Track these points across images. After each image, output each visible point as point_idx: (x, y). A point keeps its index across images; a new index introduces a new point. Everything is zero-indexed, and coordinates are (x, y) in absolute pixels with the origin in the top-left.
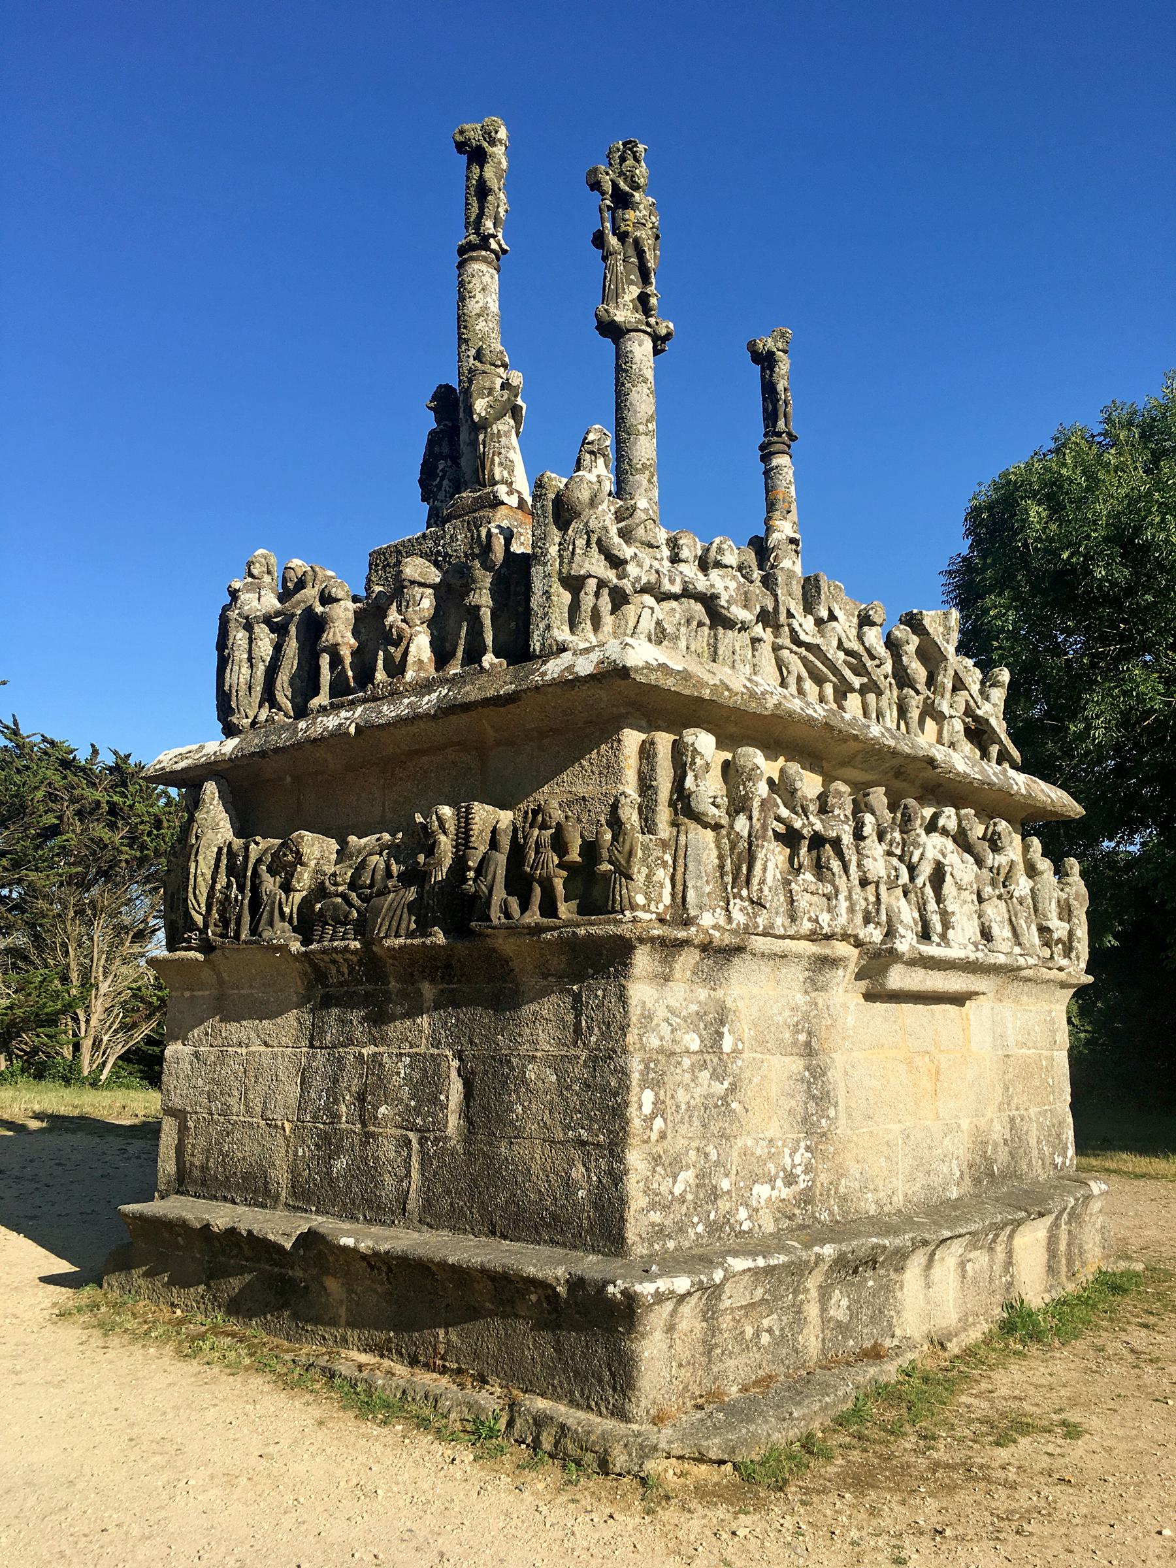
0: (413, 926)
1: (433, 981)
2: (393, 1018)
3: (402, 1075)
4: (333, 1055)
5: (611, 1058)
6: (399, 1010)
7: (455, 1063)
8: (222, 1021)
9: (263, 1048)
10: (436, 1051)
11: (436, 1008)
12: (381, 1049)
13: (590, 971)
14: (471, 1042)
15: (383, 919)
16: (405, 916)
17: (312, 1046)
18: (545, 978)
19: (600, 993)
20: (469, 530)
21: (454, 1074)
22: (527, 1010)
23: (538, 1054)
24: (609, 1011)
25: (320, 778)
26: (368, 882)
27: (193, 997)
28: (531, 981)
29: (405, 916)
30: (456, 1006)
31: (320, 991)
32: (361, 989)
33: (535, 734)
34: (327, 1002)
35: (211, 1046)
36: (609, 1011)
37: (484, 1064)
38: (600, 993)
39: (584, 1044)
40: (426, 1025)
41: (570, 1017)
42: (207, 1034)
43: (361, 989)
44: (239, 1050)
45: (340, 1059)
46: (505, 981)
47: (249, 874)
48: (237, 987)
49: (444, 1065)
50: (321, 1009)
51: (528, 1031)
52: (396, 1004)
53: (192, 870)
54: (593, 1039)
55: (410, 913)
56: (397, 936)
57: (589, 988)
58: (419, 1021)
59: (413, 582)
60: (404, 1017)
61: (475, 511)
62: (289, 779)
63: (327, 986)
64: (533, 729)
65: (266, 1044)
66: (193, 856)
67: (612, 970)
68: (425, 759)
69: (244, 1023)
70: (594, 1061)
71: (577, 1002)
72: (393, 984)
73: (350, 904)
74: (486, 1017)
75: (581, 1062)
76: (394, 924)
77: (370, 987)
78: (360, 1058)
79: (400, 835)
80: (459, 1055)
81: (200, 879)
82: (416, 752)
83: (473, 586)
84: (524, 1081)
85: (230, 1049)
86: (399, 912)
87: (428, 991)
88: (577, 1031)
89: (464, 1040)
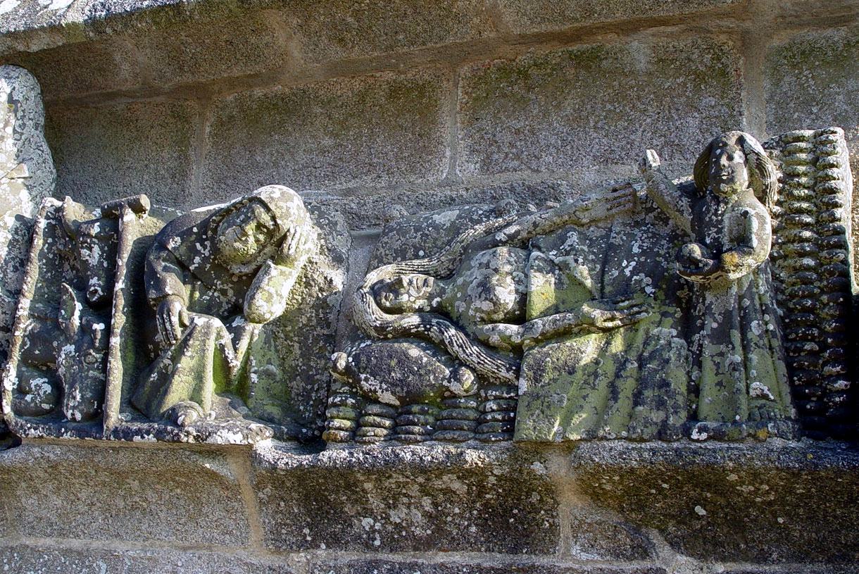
73: (456, 363)
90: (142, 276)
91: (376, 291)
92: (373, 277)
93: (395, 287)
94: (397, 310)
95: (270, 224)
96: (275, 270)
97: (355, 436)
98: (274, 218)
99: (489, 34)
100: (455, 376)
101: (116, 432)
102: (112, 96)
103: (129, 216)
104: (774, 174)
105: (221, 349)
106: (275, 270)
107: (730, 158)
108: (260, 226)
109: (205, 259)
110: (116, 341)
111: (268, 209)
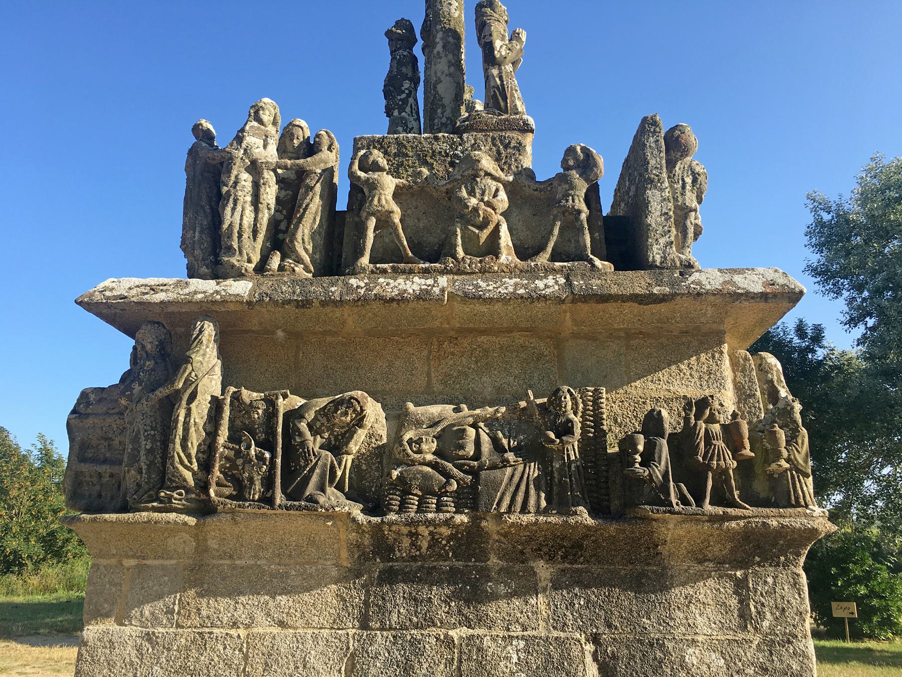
0: (544, 504)
1: (551, 559)
2: (494, 597)
3: (515, 659)
4: (403, 637)
5: (789, 642)
6: (502, 589)
7: (589, 648)
8: (200, 595)
9: (276, 630)
10: (562, 635)
11: (556, 586)
12: (478, 631)
13: (757, 559)
14: (610, 626)
15: (503, 494)
16: (532, 492)
17: (364, 626)
18: (700, 562)
19: (770, 580)
20: (494, 145)
21: (589, 659)
22: (677, 593)
23: (700, 638)
24: (783, 598)
25: (329, 339)
26: (472, 453)
27: (140, 568)
28: (679, 565)
29: (532, 492)
30: (586, 586)
31: (379, 565)
32: (445, 565)
33: (622, 334)
34: (389, 577)
35: (179, 626)
36: (783, 598)
37: (628, 647)
38: (770, 580)
39: (756, 629)
40: (543, 607)
41: (734, 602)
42: (172, 612)
43: (445, 565)
44: (233, 632)
45: (414, 642)
46: (648, 564)
47: (280, 430)
48: (231, 557)
49: (575, 651)
50: (380, 585)
51: (681, 615)
52: (498, 582)
53: (181, 418)
54: (766, 624)
55: (538, 489)
56: (524, 510)
57: (755, 573)
58: (533, 601)
59: (488, 174)
60: (509, 596)
61: (502, 130)
62: (280, 334)
63: (392, 560)
64: (620, 329)
65: (282, 624)
66: (184, 403)
67: (782, 558)
68: (483, 339)
69: (242, 599)
70: (770, 645)
71: (740, 586)
72: (494, 561)
73: (448, 476)
74: (626, 599)
75: (754, 646)
76: (520, 499)
77: (460, 564)
78: (449, 642)
79: (503, 409)
80: (595, 639)
81: (192, 429)
82: (470, 331)
83: (572, 192)
84: (683, 665)
85: (216, 630)
86: (523, 487)
87: (543, 570)
88: (744, 615)
89: (600, 623)
90: (290, 431)
91: (410, 442)
92: (407, 436)
93: (419, 441)
94: (420, 451)
95: (359, 409)
96: (360, 431)
97: (403, 507)
98: (361, 407)
99: (446, 326)
100: (448, 483)
101: (280, 506)
102: (246, 332)
103: (281, 400)
104: (581, 406)
105: (332, 467)
106: (360, 431)
107: (565, 398)
108: (355, 410)
109: (323, 424)
110: (279, 461)
111: (359, 403)
